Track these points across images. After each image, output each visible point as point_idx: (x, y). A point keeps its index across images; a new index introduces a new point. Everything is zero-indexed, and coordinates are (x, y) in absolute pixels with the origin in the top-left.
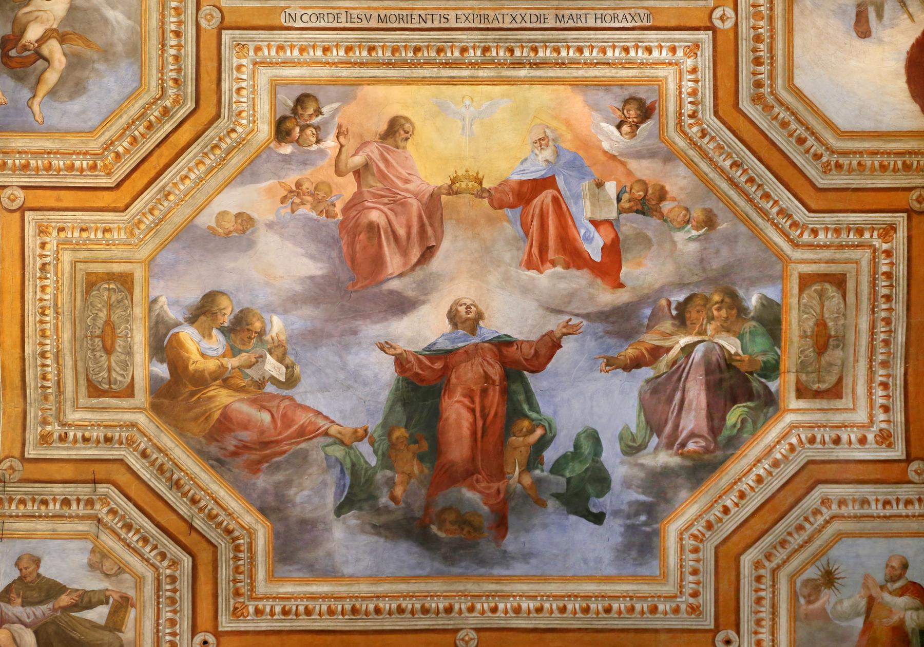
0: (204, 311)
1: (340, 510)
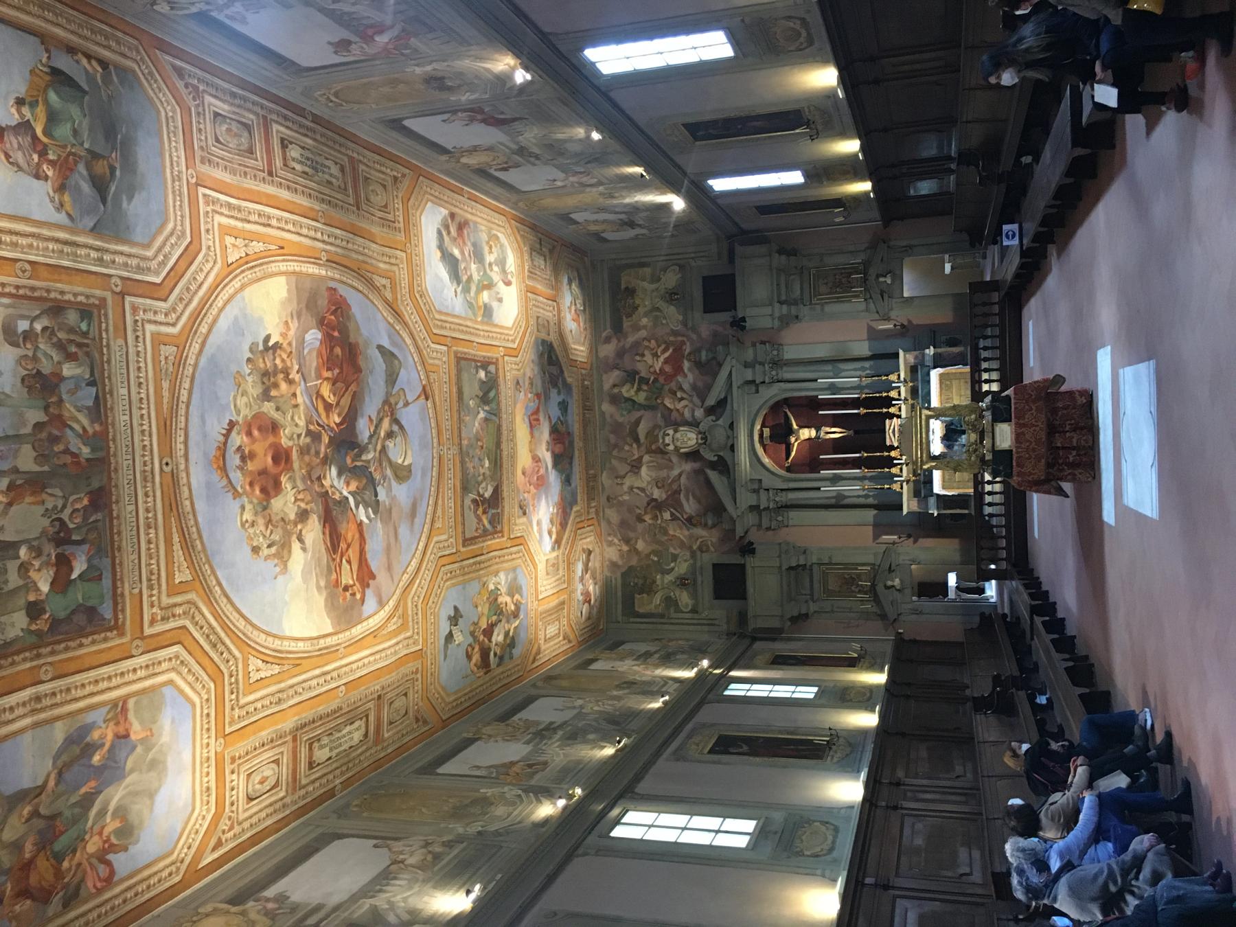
0: (550, 533)
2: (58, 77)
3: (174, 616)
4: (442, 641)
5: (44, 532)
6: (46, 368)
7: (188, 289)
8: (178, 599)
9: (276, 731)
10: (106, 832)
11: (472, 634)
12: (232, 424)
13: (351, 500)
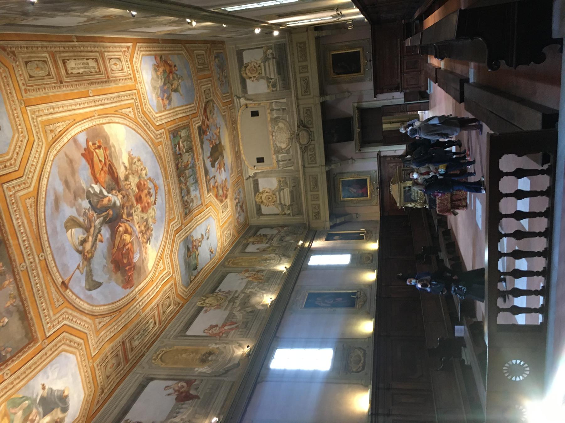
12: (155, 203)
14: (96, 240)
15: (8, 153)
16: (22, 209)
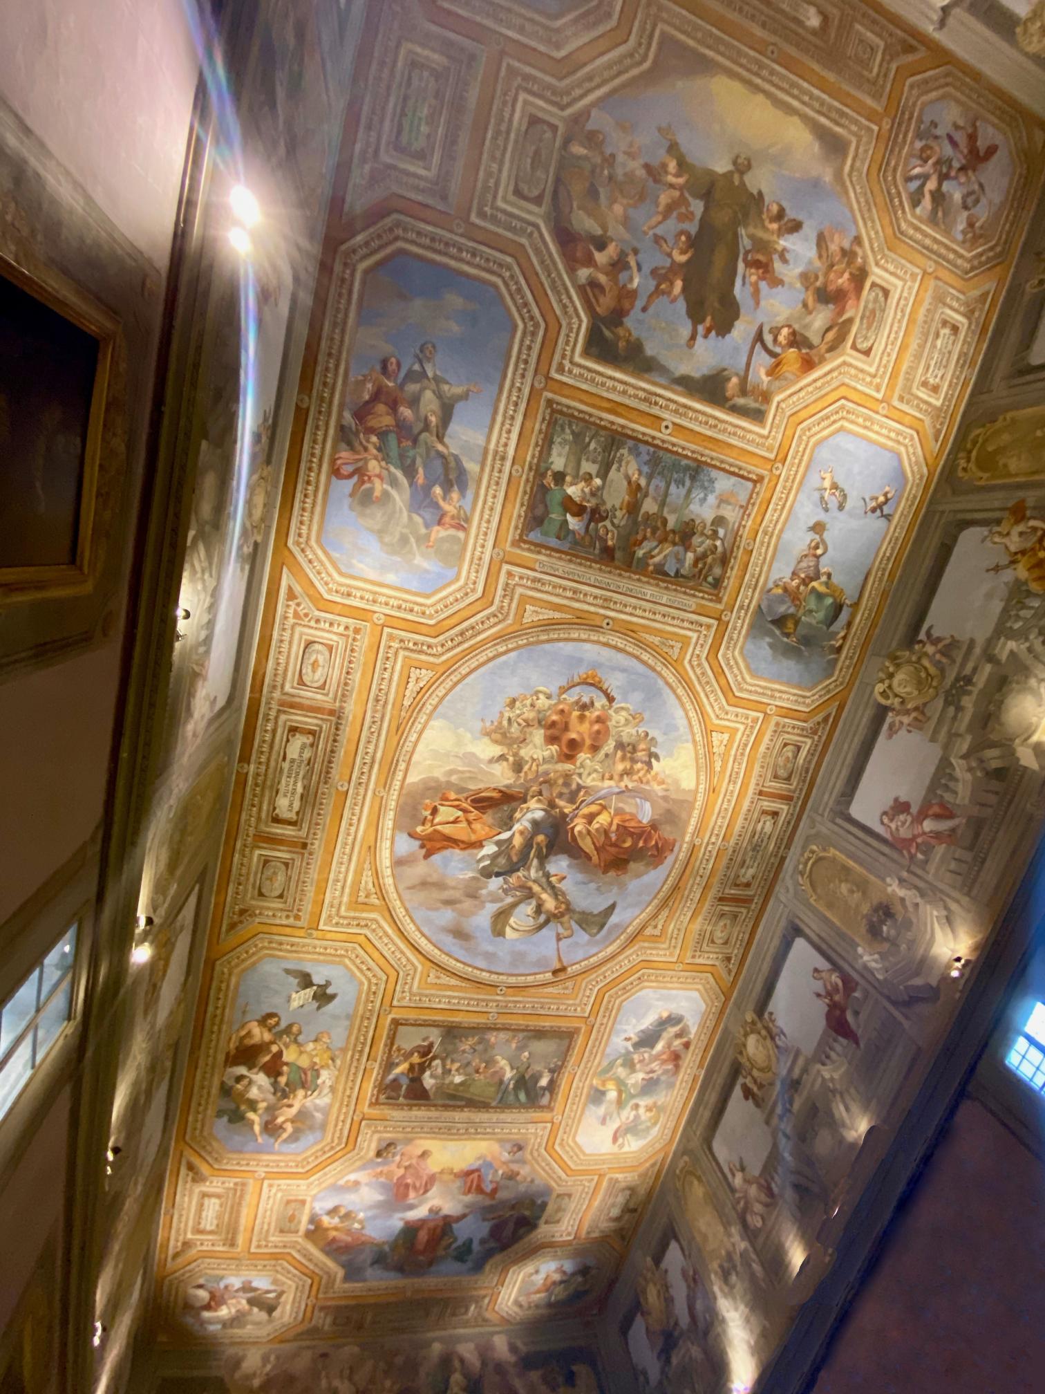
1: (373, 1264)
2: (838, 608)
3: (505, 596)
4: (308, 968)
5: (604, 503)
6: (696, 540)
7: (708, 683)
8: (514, 605)
9: (353, 689)
10: (377, 482)
11: (288, 1030)
12: (611, 700)
13: (505, 836)
14: (553, 887)
15: (362, 984)
16: (433, 992)
